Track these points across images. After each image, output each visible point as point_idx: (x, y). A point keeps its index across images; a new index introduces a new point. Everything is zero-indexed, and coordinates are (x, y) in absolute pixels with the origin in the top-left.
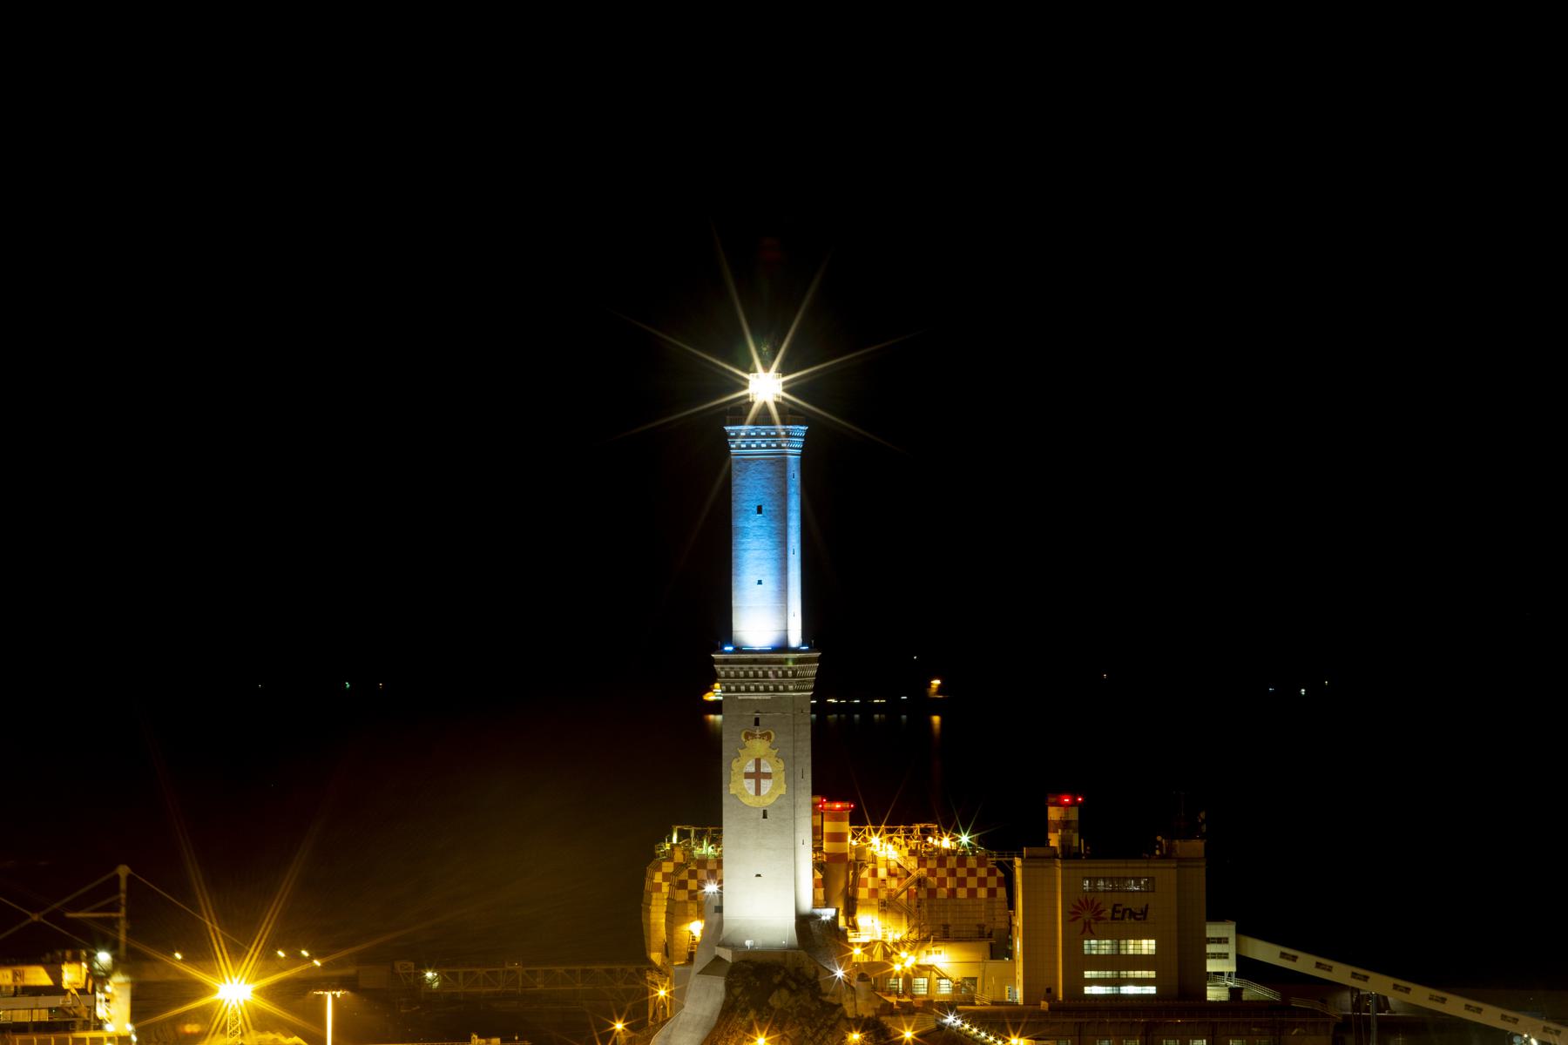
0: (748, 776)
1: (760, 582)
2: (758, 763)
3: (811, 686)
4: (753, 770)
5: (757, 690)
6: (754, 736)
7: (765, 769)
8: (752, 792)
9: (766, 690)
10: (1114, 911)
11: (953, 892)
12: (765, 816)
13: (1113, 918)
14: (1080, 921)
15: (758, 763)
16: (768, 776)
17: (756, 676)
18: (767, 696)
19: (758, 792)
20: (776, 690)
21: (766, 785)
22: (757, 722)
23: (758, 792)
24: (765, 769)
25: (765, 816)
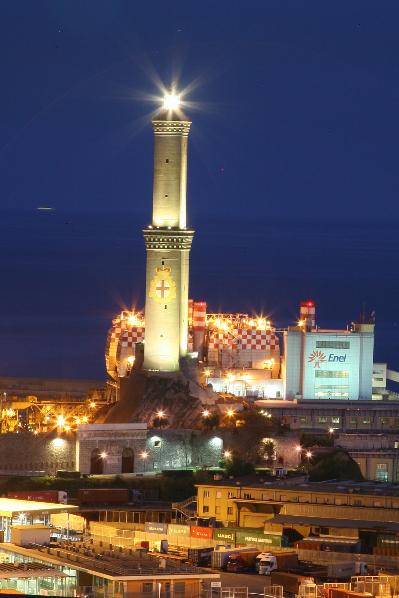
0: (158, 288)
1: (166, 196)
2: (163, 282)
3: (190, 247)
4: (161, 286)
5: (164, 248)
6: (161, 270)
7: (166, 285)
8: (160, 296)
9: (168, 248)
10: (330, 357)
11: (254, 347)
12: (166, 308)
13: (329, 361)
14: (314, 362)
15: (163, 282)
16: (167, 289)
17: (163, 241)
18: (168, 250)
20: (173, 248)
25: (166, 308)
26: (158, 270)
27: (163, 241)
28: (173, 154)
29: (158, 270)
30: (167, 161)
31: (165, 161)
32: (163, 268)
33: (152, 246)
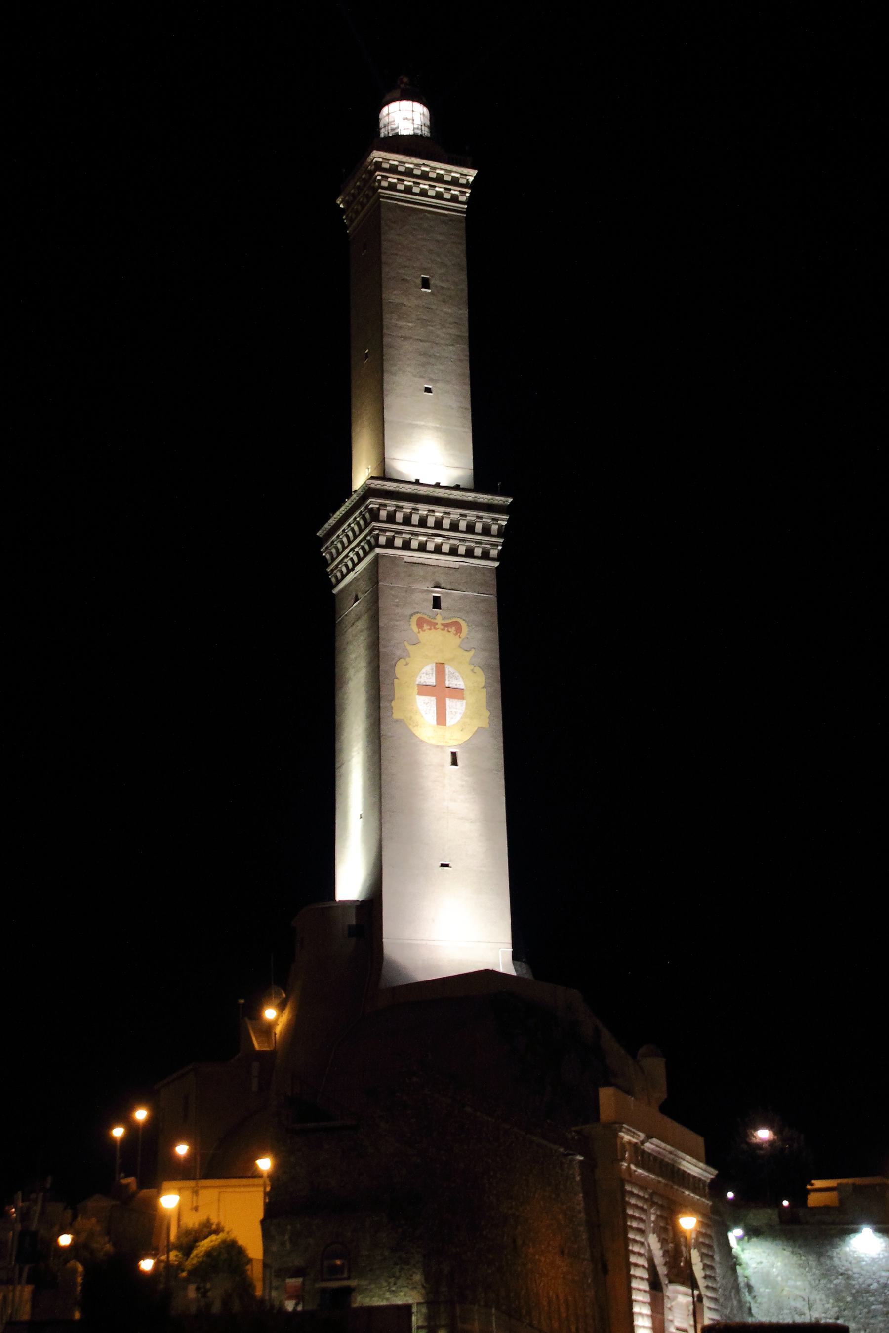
0: (424, 690)
1: (428, 390)
4: (432, 681)
5: (438, 550)
6: (433, 625)
9: (453, 552)
12: (455, 762)
15: (440, 669)
16: (457, 693)
19: (441, 718)
20: (469, 553)
21: (456, 709)
22: (437, 603)
23: (441, 718)
24: (454, 681)
25: (455, 762)
26: (420, 624)
27: (438, 525)
28: (443, 265)
29: (420, 624)
30: (426, 284)
31: (419, 282)
32: (439, 620)
33: (398, 542)
